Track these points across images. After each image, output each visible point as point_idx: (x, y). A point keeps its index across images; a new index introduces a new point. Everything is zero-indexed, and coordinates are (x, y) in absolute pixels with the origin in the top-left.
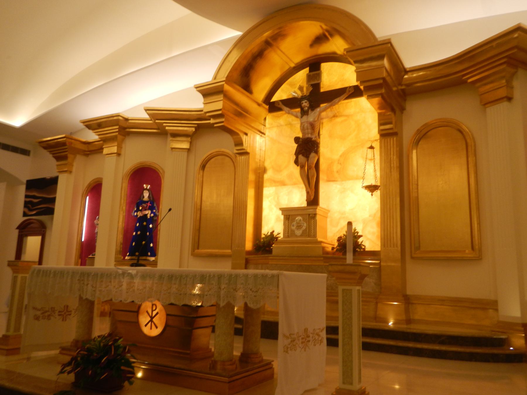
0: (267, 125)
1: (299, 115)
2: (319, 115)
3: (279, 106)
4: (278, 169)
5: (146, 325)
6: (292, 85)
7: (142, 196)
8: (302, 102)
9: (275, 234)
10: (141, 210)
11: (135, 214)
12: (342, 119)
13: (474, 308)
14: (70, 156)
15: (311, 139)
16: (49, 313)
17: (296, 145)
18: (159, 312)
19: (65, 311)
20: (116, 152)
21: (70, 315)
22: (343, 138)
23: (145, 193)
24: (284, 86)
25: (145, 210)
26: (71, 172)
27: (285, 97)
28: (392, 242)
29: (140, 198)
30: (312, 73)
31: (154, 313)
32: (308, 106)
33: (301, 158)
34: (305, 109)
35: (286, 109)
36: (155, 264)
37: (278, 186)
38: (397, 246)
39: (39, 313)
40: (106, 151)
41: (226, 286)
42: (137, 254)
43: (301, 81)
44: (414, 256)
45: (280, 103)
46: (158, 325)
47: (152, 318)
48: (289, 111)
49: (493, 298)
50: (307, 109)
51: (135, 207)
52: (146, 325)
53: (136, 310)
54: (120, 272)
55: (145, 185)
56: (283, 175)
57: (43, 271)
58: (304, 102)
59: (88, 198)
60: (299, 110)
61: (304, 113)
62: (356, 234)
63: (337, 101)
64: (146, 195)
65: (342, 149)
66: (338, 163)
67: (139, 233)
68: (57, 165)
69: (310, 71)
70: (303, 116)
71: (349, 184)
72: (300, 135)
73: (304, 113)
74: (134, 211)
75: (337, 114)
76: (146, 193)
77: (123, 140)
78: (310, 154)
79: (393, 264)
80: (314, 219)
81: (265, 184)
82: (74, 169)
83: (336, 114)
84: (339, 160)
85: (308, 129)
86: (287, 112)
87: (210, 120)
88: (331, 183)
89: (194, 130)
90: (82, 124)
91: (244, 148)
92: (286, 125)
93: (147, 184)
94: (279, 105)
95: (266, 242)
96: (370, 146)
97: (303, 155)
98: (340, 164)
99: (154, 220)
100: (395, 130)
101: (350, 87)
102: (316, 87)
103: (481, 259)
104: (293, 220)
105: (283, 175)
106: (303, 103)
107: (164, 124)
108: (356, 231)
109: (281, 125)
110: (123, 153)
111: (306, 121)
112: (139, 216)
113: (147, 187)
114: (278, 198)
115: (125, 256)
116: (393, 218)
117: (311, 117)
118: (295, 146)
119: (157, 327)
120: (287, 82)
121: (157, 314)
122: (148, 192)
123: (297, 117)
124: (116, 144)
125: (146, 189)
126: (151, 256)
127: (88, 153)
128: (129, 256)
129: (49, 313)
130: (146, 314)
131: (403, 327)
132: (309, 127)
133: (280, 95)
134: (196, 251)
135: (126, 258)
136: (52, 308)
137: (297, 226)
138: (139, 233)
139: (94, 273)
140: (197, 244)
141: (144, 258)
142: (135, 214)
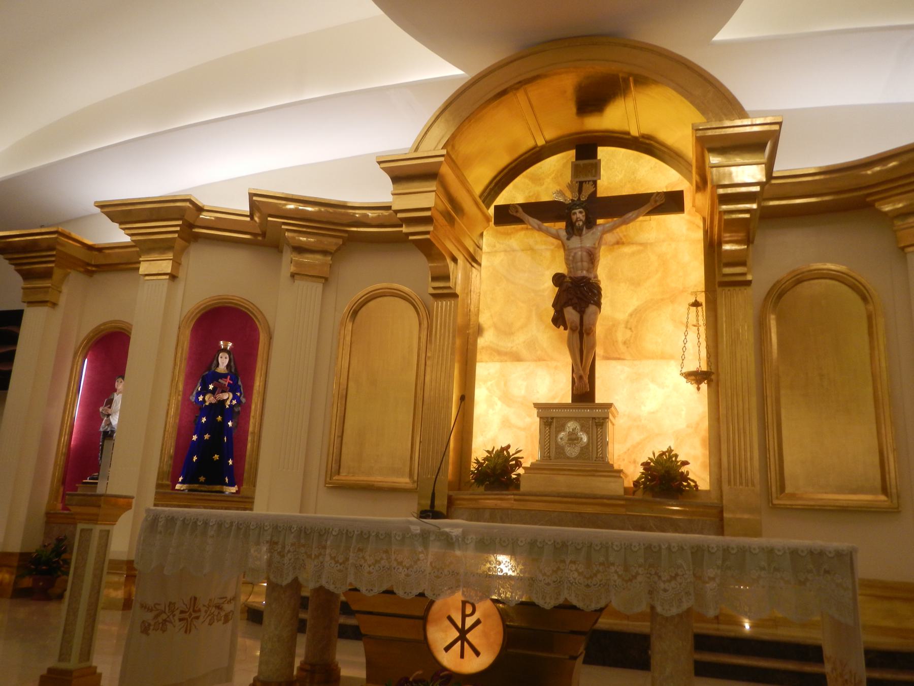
0: (485, 248)
1: (563, 234)
2: (601, 238)
3: (518, 215)
4: (506, 331)
5: (447, 649)
6: (536, 180)
7: (215, 362)
8: (573, 211)
9: (512, 451)
10: (213, 392)
11: (201, 398)
12: (634, 248)
13: (890, 599)
14: (58, 273)
15: (590, 279)
16: (164, 616)
17: (557, 289)
18: (482, 620)
19: (191, 610)
20: (169, 271)
21: (197, 618)
22: (635, 283)
23: (221, 357)
24: (519, 180)
25: (223, 392)
26: (54, 305)
27: (520, 199)
28: (743, 476)
29: (209, 368)
30: (581, 162)
31: (469, 622)
32: (584, 219)
33: (571, 314)
34: (577, 224)
35: (534, 222)
36: (246, 502)
37: (506, 361)
38: (753, 485)
39: (149, 617)
40: (144, 268)
41: (719, 572)
42: (202, 479)
43: (553, 175)
44: (776, 502)
45: (520, 209)
46: (479, 649)
47: (463, 633)
48: (539, 225)
50: (582, 225)
51: (199, 385)
52: (447, 649)
53: (419, 612)
54: (456, 532)
55: (222, 343)
56: (518, 342)
57: (184, 520)
58: (577, 211)
59: (86, 360)
60: (562, 225)
61: (573, 230)
62: (674, 459)
63: (634, 216)
64: (223, 361)
65: (634, 303)
66: (626, 327)
67: (207, 437)
68: (23, 288)
69: (578, 157)
70: (571, 237)
71: (646, 366)
73: (573, 230)
74: (195, 393)
75: (624, 240)
76: (224, 358)
77: (184, 250)
78: (587, 306)
79: (746, 516)
80: (602, 428)
81: (479, 357)
82: (63, 300)
83: (621, 239)
84: (627, 322)
85: (582, 261)
86: (536, 226)
87: (401, 226)
88: (613, 363)
89: (341, 243)
90: (98, 210)
91: (451, 284)
92: (523, 250)
93: (227, 340)
94: (517, 212)
95: (497, 467)
96: (692, 300)
97: (575, 308)
98: (630, 329)
99: (240, 412)
100: (749, 277)
101: (658, 193)
103: (899, 512)
104: (562, 428)
105: (518, 342)
106: (575, 213)
107: (283, 227)
108: (673, 453)
109: (514, 251)
110: (181, 274)
111: (580, 246)
112: (207, 404)
113: (226, 346)
114: (506, 384)
115: (175, 482)
116: (745, 433)
117: (588, 240)
119: (477, 654)
120: (524, 173)
121: (478, 622)
122: (227, 356)
123: (557, 237)
124: (170, 255)
125: (225, 350)
126: (231, 484)
127: (94, 269)
129: (164, 616)
130: (448, 623)
131: (768, 634)
132: (586, 257)
133: (513, 195)
134: (334, 478)
135: (178, 486)
136: (170, 603)
137: (569, 440)
138: (207, 437)
139: (337, 529)
141: (218, 488)
142: (201, 398)
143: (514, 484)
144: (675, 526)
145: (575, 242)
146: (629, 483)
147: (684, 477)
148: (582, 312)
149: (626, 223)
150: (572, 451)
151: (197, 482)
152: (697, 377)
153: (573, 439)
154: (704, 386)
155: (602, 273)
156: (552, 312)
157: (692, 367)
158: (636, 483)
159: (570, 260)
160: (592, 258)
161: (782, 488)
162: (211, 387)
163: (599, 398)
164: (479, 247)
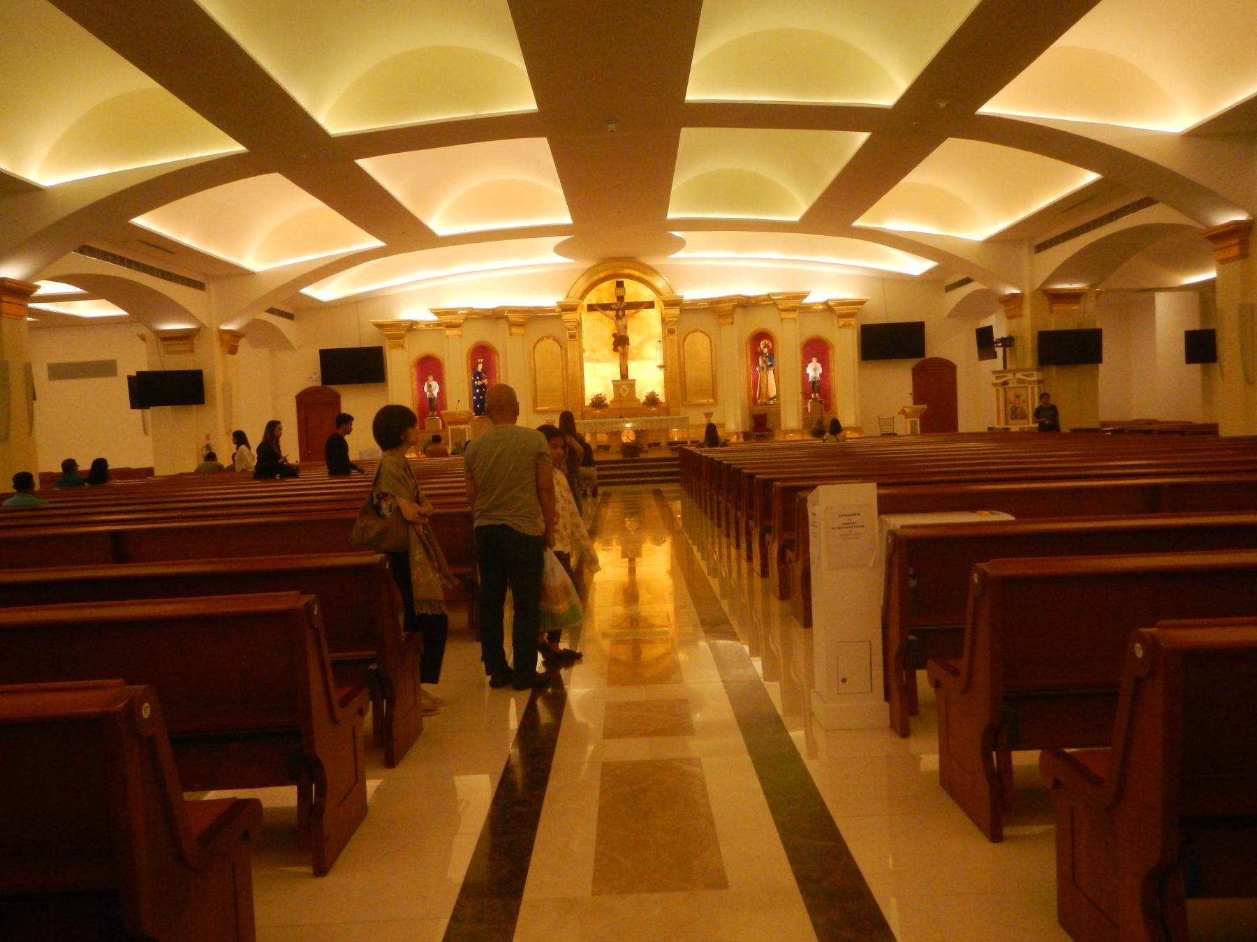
1: (615, 318)
4: (594, 351)
6: (601, 291)
10: (480, 379)
24: (594, 291)
26: (403, 347)
33: (620, 348)
49: (722, 422)
64: (480, 367)
72: (615, 332)
73: (618, 317)
82: (406, 345)
102: (621, 298)
118: (613, 339)
123: (613, 319)
128: (476, 415)
133: (592, 298)
140: (535, 404)
143: (606, 406)
144: (655, 414)
145: (620, 322)
146: (642, 401)
147: (658, 399)
148: (623, 347)
149: (636, 313)
150: (624, 395)
151: (481, 414)
152: (661, 367)
153: (624, 391)
154: (663, 369)
155: (630, 334)
156: (612, 347)
157: (659, 364)
158: (644, 403)
159: (617, 326)
160: (626, 328)
161: (686, 400)
162: (478, 378)
163: (629, 378)
164: (581, 319)
